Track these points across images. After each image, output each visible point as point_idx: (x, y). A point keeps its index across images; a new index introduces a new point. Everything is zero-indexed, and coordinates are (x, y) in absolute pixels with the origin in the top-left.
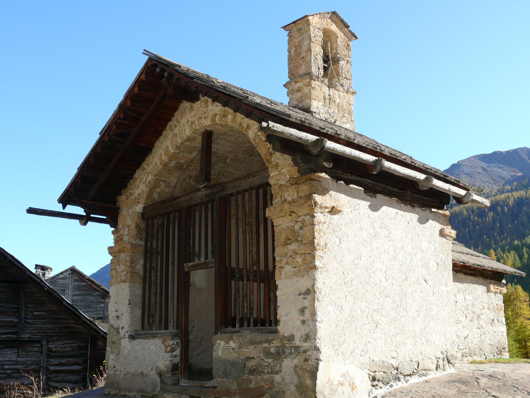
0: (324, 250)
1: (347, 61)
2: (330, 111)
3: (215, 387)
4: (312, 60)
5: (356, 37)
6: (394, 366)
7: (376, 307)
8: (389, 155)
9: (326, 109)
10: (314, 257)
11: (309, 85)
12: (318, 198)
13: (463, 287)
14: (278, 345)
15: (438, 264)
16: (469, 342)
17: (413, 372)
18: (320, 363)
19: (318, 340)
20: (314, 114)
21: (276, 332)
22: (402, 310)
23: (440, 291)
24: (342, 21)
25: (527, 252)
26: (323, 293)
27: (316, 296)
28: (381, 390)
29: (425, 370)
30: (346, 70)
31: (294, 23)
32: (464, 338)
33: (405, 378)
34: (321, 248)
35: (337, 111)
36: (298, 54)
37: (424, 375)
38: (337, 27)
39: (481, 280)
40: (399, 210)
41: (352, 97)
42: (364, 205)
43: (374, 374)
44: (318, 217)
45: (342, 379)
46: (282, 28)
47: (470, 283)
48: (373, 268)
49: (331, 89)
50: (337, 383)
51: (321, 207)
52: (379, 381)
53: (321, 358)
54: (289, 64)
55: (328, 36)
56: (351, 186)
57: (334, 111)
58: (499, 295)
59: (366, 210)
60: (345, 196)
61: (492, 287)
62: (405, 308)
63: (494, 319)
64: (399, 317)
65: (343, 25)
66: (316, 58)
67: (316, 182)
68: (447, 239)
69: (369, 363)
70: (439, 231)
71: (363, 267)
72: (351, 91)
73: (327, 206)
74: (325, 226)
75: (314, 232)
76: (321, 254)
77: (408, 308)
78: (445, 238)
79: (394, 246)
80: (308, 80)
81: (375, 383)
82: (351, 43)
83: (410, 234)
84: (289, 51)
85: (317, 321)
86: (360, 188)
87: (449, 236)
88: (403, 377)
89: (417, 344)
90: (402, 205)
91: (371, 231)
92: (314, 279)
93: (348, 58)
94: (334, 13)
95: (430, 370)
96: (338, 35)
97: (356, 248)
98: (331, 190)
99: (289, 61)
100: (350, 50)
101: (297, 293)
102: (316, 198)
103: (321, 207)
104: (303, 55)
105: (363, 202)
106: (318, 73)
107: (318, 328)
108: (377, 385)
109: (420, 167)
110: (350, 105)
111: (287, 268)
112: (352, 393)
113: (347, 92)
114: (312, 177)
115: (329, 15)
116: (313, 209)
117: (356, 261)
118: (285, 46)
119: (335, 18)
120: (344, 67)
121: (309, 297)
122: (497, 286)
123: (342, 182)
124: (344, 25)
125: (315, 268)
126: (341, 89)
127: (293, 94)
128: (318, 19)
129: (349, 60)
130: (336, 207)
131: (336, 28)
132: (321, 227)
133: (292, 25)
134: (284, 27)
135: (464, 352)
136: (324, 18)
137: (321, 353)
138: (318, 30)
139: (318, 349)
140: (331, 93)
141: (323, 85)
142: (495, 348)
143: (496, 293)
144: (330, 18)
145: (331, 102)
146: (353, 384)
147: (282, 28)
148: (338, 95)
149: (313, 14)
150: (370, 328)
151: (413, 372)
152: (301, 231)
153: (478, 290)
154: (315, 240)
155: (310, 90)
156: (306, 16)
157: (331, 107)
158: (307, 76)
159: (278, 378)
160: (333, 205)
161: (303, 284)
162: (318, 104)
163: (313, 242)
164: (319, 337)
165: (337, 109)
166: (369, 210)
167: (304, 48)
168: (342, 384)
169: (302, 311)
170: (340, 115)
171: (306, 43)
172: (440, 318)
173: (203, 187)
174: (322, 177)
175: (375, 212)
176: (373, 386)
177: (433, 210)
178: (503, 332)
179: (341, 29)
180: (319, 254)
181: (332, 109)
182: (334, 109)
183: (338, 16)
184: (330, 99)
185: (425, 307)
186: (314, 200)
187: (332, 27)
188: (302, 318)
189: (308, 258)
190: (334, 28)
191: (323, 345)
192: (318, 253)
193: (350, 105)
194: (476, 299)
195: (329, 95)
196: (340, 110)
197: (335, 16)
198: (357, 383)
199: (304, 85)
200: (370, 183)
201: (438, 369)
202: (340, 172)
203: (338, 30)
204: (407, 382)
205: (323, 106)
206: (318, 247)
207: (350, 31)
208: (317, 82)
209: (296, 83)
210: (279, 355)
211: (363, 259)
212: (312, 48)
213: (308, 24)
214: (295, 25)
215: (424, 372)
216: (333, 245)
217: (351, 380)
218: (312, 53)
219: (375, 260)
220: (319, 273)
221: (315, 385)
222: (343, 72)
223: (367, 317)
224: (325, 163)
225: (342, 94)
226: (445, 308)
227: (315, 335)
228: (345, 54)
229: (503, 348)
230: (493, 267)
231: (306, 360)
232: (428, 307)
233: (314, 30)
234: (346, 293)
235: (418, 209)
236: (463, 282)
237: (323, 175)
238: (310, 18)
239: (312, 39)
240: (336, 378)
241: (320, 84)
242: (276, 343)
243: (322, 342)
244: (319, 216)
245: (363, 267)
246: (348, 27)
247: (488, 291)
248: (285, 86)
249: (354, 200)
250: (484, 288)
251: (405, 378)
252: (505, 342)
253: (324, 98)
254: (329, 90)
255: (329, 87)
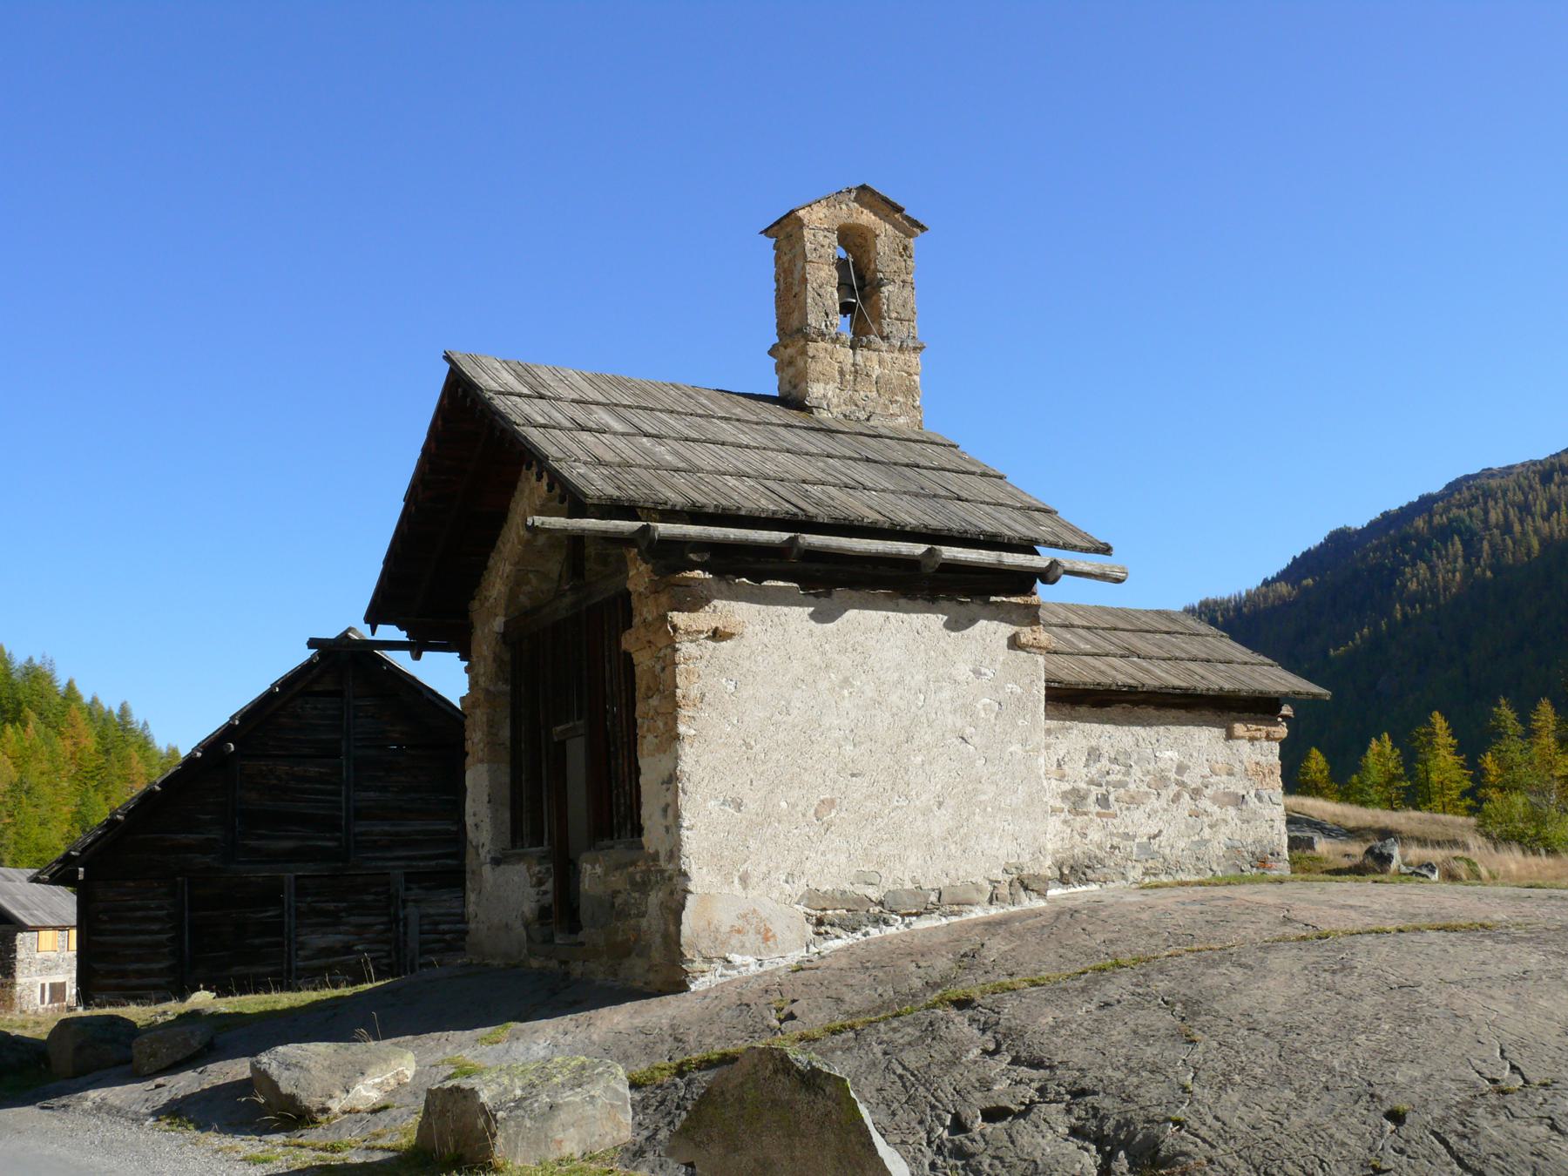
0: (699, 705)
1: (903, 281)
2: (856, 396)
3: (582, 944)
4: (809, 300)
5: (923, 228)
6: (874, 899)
7: (828, 796)
8: (831, 522)
9: (846, 395)
10: (675, 719)
11: (804, 352)
12: (679, 618)
13: (1152, 733)
14: (644, 868)
15: (1000, 704)
16: (1162, 844)
17: (926, 909)
18: (689, 897)
19: (684, 859)
20: (814, 410)
21: (641, 847)
22: (897, 798)
23: (1007, 757)
24: (886, 201)
25: (1336, 649)
26: (695, 779)
27: (680, 785)
28: (837, 941)
29: (958, 904)
30: (900, 302)
31: (778, 223)
32: (1149, 839)
33: (903, 920)
34: (690, 704)
35: (874, 394)
36: (789, 287)
37: (953, 913)
38: (875, 214)
39: (1208, 714)
40: (894, 611)
41: (915, 359)
42: (797, 617)
43: (823, 913)
44: (684, 649)
45: (739, 924)
46: (761, 233)
47: (1173, 724)
48: (820, 725)
49: (858, 351)
50: (728, 929)
51: (687, 633)
52: (832, 925)
53: (691, 887)
54: (778, 307)
55: (852, 238)
56: (765, 583)
57: (867, 396)
58: (1265, 744)
59: (804, 623)
60: (748, 605)
61: (1239, 728)
62: (905, 793)
63: (1245, 793)
64: (886, 811)
65: (887, 209)
66: (819, 295)
67: (681, 589)
68: (1028, 652)
69: (807, 895)
70: (1009, 638)
71: (794, 726)
72: (911, 345)
73: (701, 629)
74: (701, 664)
75: (675, 677)
76: (690, 714)
77: (914, 793)
78: (1024, 650)
79: (877, 681)
80: (802, 343)
81: (822, 930)
82: (912, 242)
83: (923, 655)
84: (777, 281)
85: (681, 826)
86: (790, 584)
87: (1032, 646)
88: (899, 919)
89: (934, 858)
90: (902, 602)
91: (817, 659)
92: (677, 758)
93: (903, 276)
94: (863, 188)
95: (971, 904)
96: (877, 232)
97: (775, 695)
98: (715, 598)
99: (776, 302)
100: (910, 257)
101: (660, 781)
102: (675, 619)
103: (687, 633)
104: (796, 289)
105: (797, 608)
106: (823, 324)
107: (685, 839)
108: (827, 933)
109: (917, 530)
110: (911, 375)
111: (650, 737)
112: (762, 946)
113: (901, 349)
114: (672, 581)
115: (853, 195)
116: (672, 637)
117: (777, 717)
118: (771, 270)
119: (867, 198)
120: (892, 298)
121: (671, 786)
122: (1257, 724)
123: (744, 579)
124: (888, 208)
125: (676, 737)
126: (884, 346)
127: (783, 371)
128: (825, 210)
129: (909, 278)
130: (721, 628)
131: (873, 217)
132: (692, 666)
133: (776, 228)
134: (765, 232)
135: (1148, 865)
136: (840, 203)
137: (690, 880)
138: (826, 233)
139: (685, 875)
140: (859, 359)
141: (838, 346)
142: (1245, 854)
143: (1252, 739)
144: (856, 200)
145: (859, 379)
146: (767, 930)
147: (761, 233)
148: (877, 362)
149: (808, 202)
150: (811, 834)
151: (926, 909)
152: (662, 675)
153: (1196, 736)
154: (678, 691)
155: (806, 362)
156: (792, 212)
157: (858, 388)
158: (800, 335)
159: (644, 923)
160: (714, 625)
161: (664, 764)
162: (825, 389)
163: (674, 694)
164: (687, 853)
165: (875, 389)
166: (813, 623)
167: (797, 275)
168: (739, 932)
169: (665, 810)
170: (884, 400)
171: (800, 264)
172: (1003, 805)
173: (569, 590)
174: (693, 579)
175: (825, 625)
176: (818, 934)
177: (993, 599)
178: (1272, 820)
179: (885, 218)
180: (686, 713)
181: (862, 393)
182: (866, 392)
183: (874, 193)
184: (856, 372)
185: (961, 787)
186: (671, 622)
187: (864, 216)
188: (665, 823)
189: (670, 723)
190: (867, 218)
191: (694, 867)
192: (684, 713)
193: (911, 375)
194: (1191, 756)
195: (854, 365)
196: (882, 392)
197: (866, 195)
198: (777, 928)
199: (797, 352)
200: (818, 571)
201: (995, 902)
202: (750, 559)
203: (878, 220)
204: (907, 926)
205: (838, 391)
206: (683, 701)
207: (907, 218)
208: (821, 344)
209: (786, 348)
210: (643, 887)
211: (795, 712)
212: (808, 276)
213: (800, 224)
214: (782, 228)
215: (956, 908)
216: (718, 695)
217: (762, 925)
218: (809, 286)
219: (824, 711)
220: (687, 748)
221: (679, 932)
222: (892, 308)
223: (804, 815)
224: (691, 555)
225: (887, 356)
226: (1020, 787)
227: (680, 850)
228: (895, 268)
229: (1272, 854)
230: (1221, 689)
231: (672, 893)
232: (970, 787)
233: (814, 236)
234: (752, 775)
235: (945, 604)
236: (1150, 725)
237: (698, 574)
238: (801, 213)
239: (809, 255)
240: (725, 917)
241: (829, 346)
242: (641, 866)
243: (693, 862)
244: (686, 648)
245: (794, 726)
246: (900, 210)
247: (1230, 736)
248: (771, 353)
249: (772, 609)
250: (1218, 732)
251: (903, 920)
252: (1280, 840)
253: (842, 373)
254: (854, 354)
255: (853, 347)
